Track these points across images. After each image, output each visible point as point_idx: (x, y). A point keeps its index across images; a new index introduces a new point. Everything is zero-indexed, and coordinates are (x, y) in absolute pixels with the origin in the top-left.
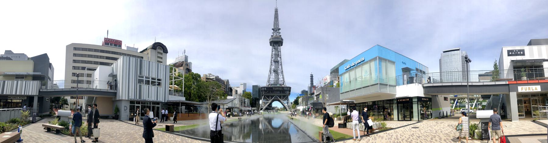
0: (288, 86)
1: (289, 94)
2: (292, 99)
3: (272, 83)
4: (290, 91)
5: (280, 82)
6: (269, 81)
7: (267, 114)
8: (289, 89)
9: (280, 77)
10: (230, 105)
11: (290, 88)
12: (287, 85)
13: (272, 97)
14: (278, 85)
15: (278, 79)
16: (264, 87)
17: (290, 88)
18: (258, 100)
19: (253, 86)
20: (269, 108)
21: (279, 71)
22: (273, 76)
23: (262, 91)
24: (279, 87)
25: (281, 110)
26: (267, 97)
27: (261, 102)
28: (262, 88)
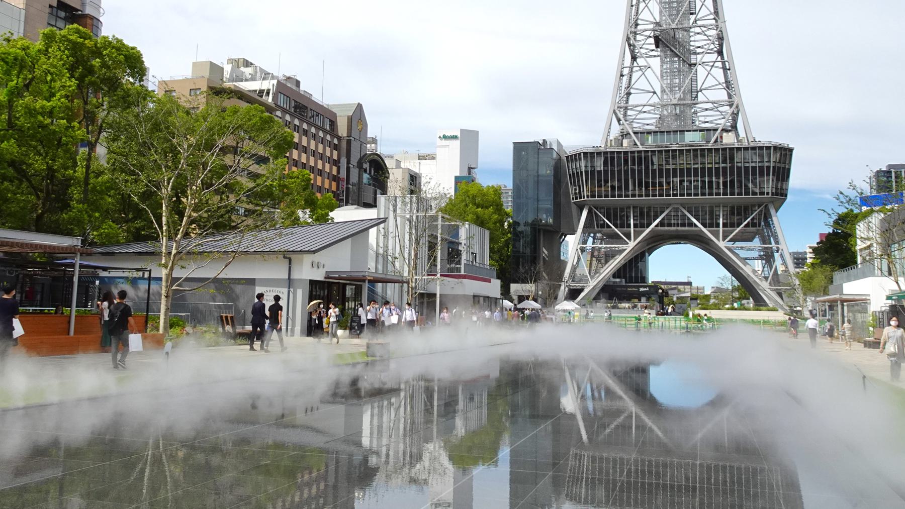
0: (765, 137)
1: (781, 194)
2: (798, 230)
3: (648, 120)
4: (782, 174)
5: (709, 117)
6: (621, 110)
7: (622, 334)
8: (779, 161)
9: (708, 77)
10: (338, 262)
11: (786, 153)
12: (761, 128)
13: (645, 216)
14: (692, 138)
15: (693, 92)
16: (590, 155)
17: (786, 153)
18: (554, 235)
19: (519, 148)
20: (627, 286)
21: (697, 40)
22: (654, 65)
23: (576, 177)
24: (698, 152)
25: (720, 299)
26: (609, 220)
27: (571, 243)
28: (574, 158)
